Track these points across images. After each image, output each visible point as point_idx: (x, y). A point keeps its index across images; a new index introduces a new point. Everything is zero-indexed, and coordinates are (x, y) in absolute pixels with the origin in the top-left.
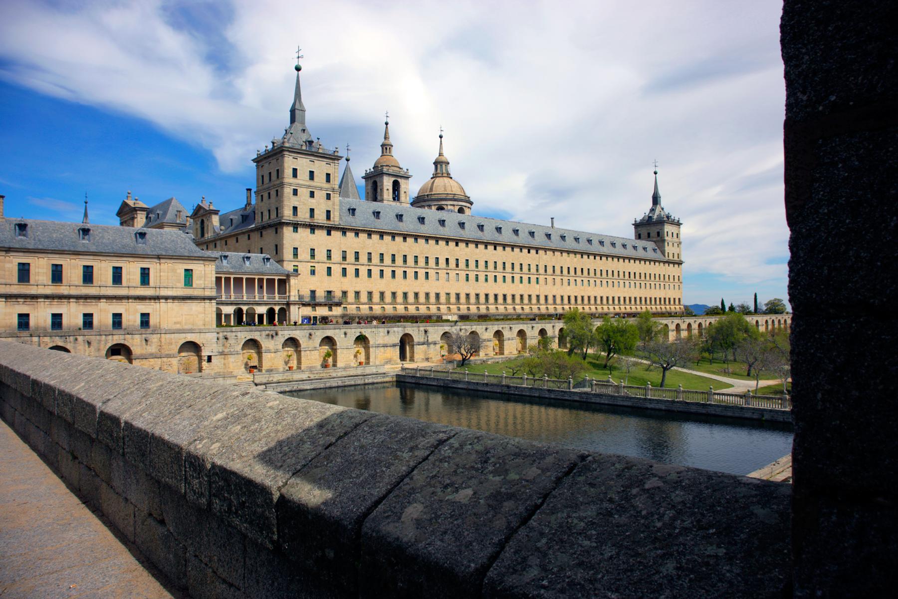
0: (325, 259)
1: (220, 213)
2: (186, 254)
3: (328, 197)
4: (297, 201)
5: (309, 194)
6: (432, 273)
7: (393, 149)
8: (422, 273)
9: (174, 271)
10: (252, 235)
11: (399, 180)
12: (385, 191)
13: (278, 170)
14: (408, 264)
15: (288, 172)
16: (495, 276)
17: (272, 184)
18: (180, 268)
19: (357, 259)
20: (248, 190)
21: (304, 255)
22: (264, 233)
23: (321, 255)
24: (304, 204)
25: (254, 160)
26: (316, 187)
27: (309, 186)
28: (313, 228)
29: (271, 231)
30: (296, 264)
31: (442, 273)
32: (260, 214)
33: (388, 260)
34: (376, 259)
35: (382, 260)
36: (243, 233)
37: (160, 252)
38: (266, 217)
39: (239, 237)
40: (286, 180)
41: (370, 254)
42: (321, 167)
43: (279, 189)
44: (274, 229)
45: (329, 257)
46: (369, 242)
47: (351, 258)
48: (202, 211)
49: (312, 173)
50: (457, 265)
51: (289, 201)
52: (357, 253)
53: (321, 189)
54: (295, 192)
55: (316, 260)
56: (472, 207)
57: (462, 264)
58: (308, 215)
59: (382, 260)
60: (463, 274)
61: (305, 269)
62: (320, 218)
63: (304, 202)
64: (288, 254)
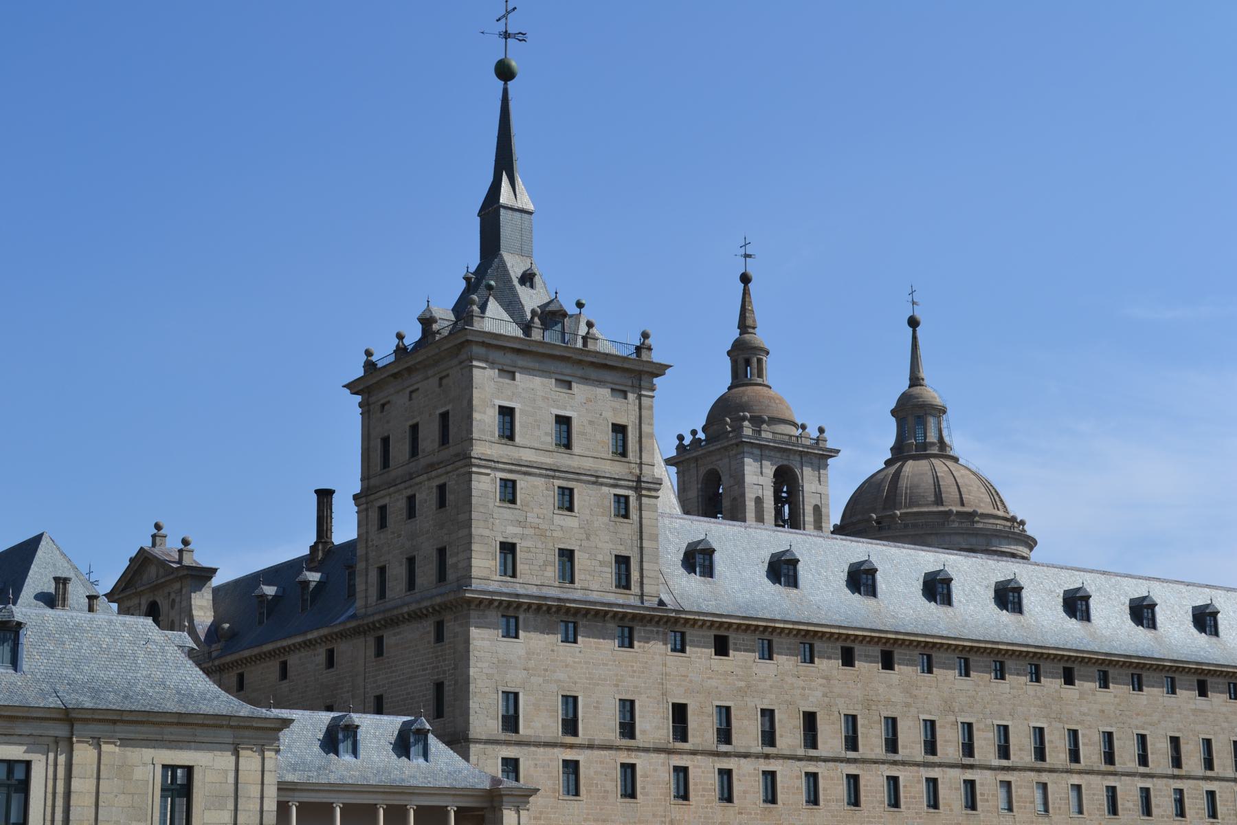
0: (612, 733)
1: (216, 581)
2: (171, 707)
3: (622, 507)
4: (514, 530)
5: (552, 498)
6: (986, 782)
7: (769, 363)
8: (951, 783)
9: (124, 771)
10: (343, 649)
11: (794, 463)
12: (750, 506)
13: (445, 417)
14: (903, 753)
15: (485, 420)
16: (1211, 795)
17: (423, 461)
18: (147, 764)
19: (725, 735)
20: (318, 492)
21: (540, 719)
22: (390, 639)
23: (599, 721)
24: (542, 535)
25: (353, 387)
26: (577, 475)
27: (552, 472)
28: (571, 620)
29: (417, 635)
30: (510, 752)
31: (1024, 785)
32: (373, 576)
33: (831, 739)
34: (789, 736)
35: (811, 738)
36: (308, 644)
37: (72, 700)
38: (396, 586)
39: (293, 660)
40: (479, 450)
41: (768, 714)
42: (592, 407)
43: (451, 485)
44: (429, 626)
45: (628, 729)
46: (766, 670)
47: (702, 729)
48: (152, 571)
49: (564, 422)
50: (1075, 756)
51: (490, 522)
52: (725, 713)
53: (596, 480)
54: (509, 491)
55: (583, 735)
56: (1034, 555)
57: (1091, 753)
59: (811, 738)
60: (1095, 788)
61: (541, 768)
62: (595, 584)
63: (535, 525)
64: (484, 717)
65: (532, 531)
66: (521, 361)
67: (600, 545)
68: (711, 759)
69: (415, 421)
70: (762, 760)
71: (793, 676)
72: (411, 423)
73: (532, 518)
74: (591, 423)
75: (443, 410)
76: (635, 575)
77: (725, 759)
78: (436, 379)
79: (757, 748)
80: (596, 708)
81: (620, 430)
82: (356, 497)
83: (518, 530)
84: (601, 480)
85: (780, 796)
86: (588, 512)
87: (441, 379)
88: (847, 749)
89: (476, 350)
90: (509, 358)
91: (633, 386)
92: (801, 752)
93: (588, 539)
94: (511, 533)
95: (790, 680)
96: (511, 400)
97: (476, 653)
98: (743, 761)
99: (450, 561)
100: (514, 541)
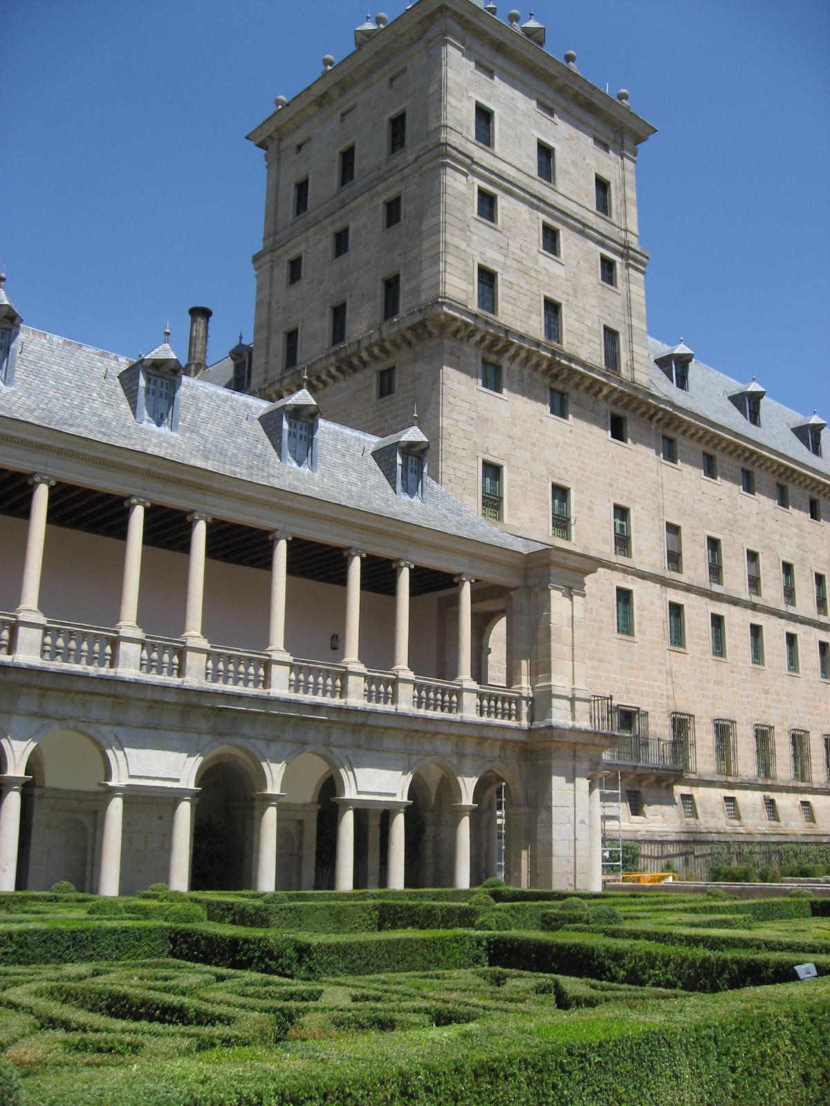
28: (561, 387)
44: (369, 378)
49: (545, 153)
53: (583, 230)
54: (487, 205)
58: (534, 326)
65: (514, 264)
66: (500, 61)
67: (588, 307)
68: (704, 600)
69: (349, 143)
70: (749, 611)
71: (772, 518)
72: (342, 147)
73: (514, 247)
74: (574, 163)
75: (393, 113)
76: (624, 357)
77: (718, 604)
78: (386, 81)
79: (744, 593)
80: (590, 509)
81: (602, 186)
82: (256, 259)
83: (500, 258)
84: (588, 230)
85: (767, 657)
86: (574, 263)
87: (392, 80)
88: (819, 613)
89: (452, 24)
90: (487, 53)
91: (615, 142)
92: (783, 607)
93: (575, 296)
94: (493, 259)
95: (771, 523)
96: (489, 100)
97: (452, 400)
98: (733, 608)
99: (404, 287)
100: (495, 268)
